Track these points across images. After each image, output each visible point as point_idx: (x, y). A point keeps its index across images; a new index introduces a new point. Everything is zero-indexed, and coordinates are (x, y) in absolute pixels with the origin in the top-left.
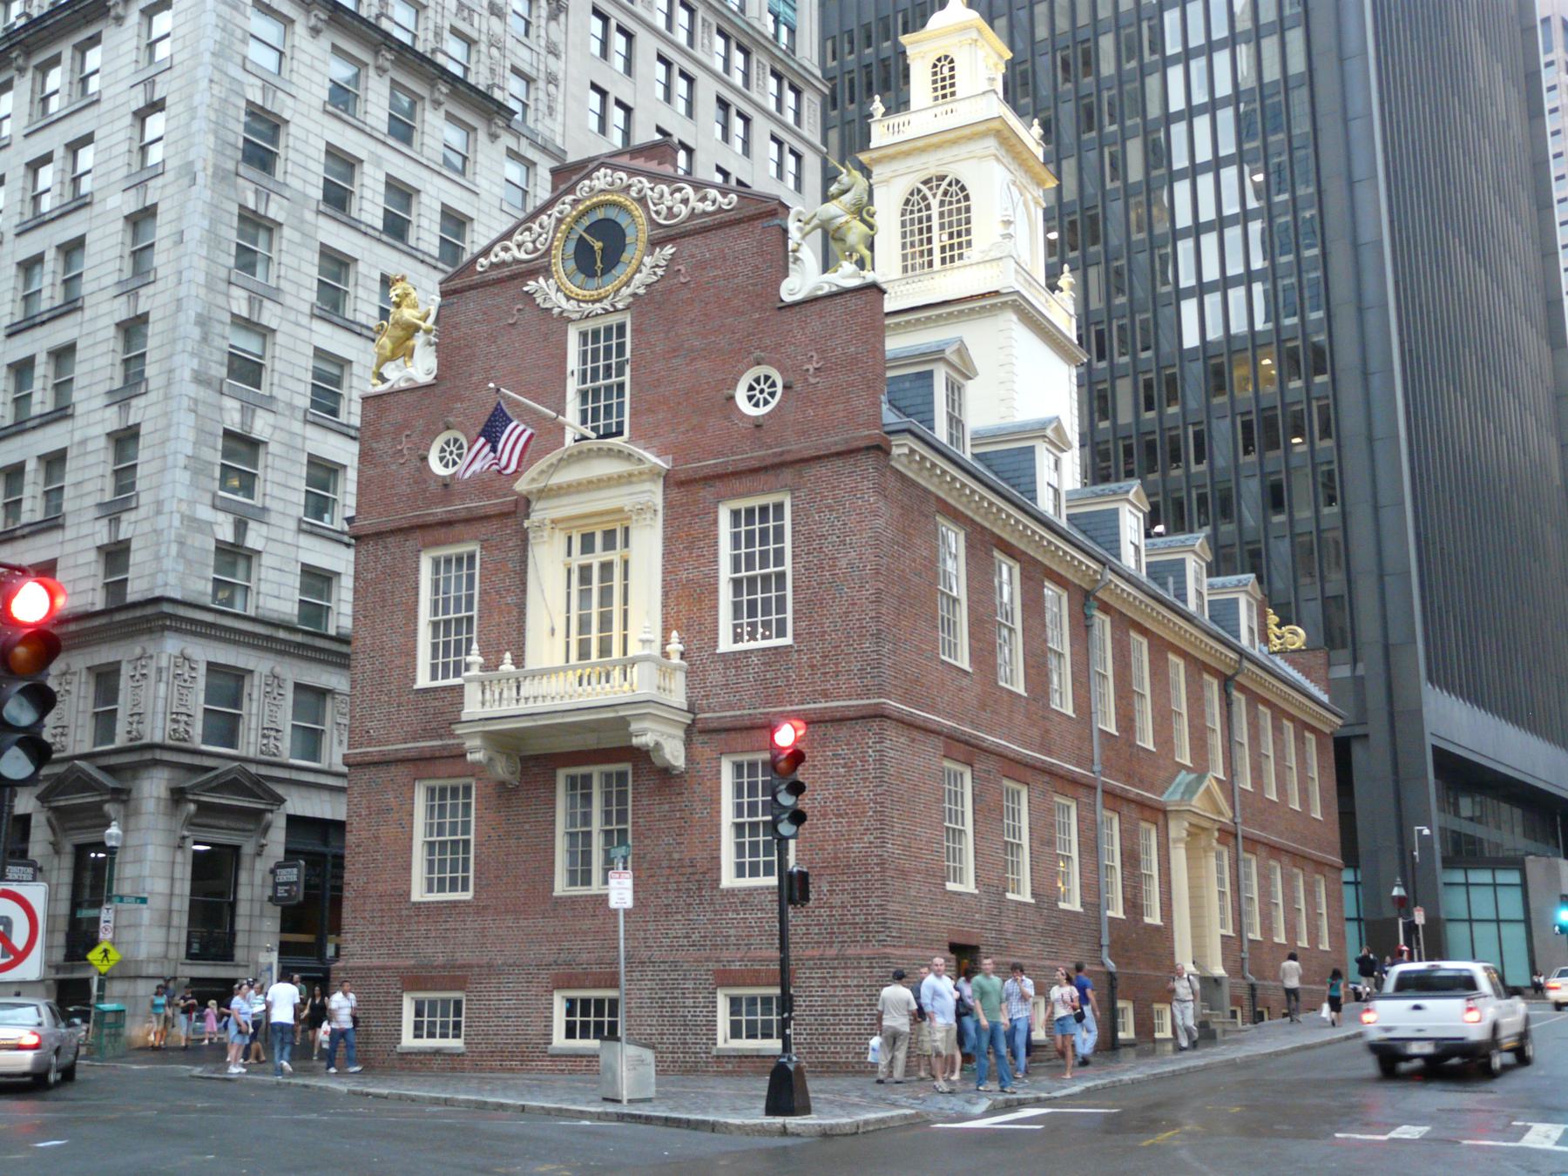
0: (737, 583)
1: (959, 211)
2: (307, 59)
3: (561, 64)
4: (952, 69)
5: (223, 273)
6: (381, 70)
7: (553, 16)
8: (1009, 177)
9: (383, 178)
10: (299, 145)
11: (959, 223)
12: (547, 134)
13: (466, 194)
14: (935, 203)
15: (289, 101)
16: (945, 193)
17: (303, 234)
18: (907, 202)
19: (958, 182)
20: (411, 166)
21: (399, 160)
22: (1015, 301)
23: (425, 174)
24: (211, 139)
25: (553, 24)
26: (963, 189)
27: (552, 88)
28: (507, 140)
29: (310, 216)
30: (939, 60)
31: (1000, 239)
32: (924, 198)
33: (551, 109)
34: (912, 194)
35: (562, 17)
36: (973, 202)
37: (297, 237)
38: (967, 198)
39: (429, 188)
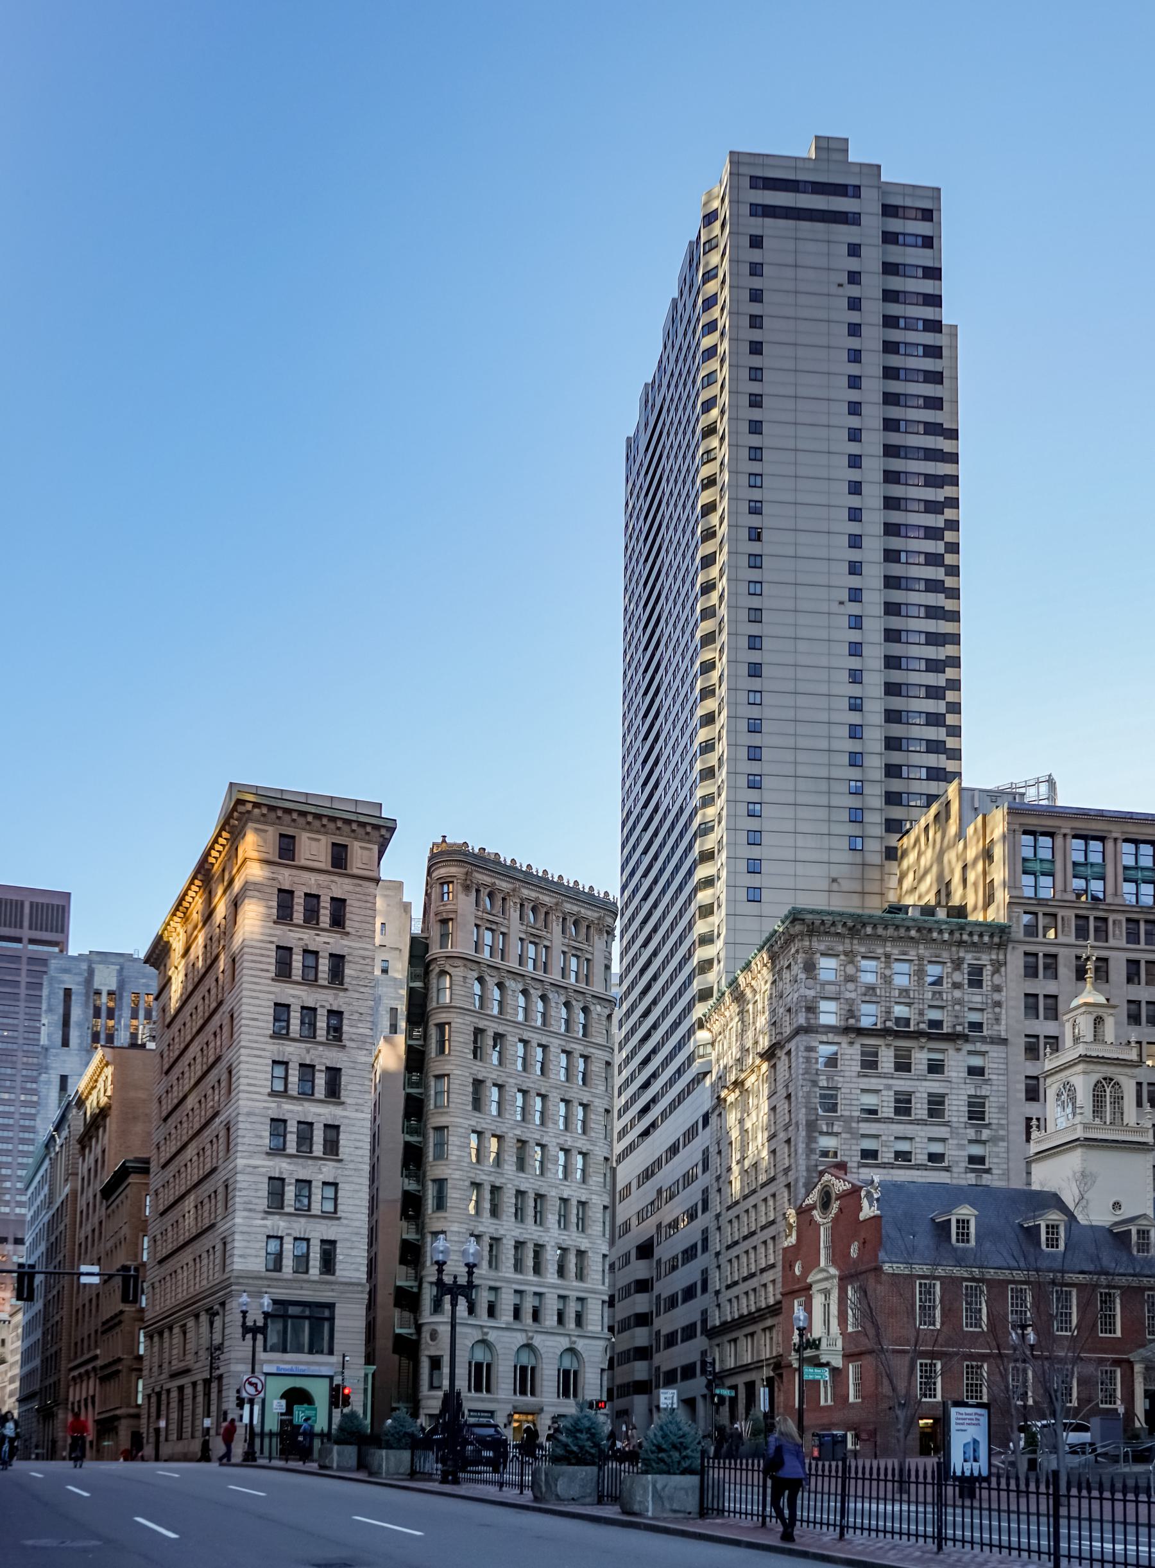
2: (848, 1057)
3: (1004, 994)
5: (813, 1163)
6: (888, 1046)
7: (996, 971)
9: (892, 1093)
10: (847, 1096)
12: (995, 1033)
13: (943, 1084)
15: (841, 1079)
17: (851, 1133)
20: (909, 1083)
21: (902, 1082)
23: (917, 1083)
24: (804, 1110)
25: (996, 976)
27: (997, 1010)
28: (969, 1047)
29: (854, 1125)
33: (997, 1019)
35: (1003, 969)
37: (848, 1136)
39: (920, 1089)
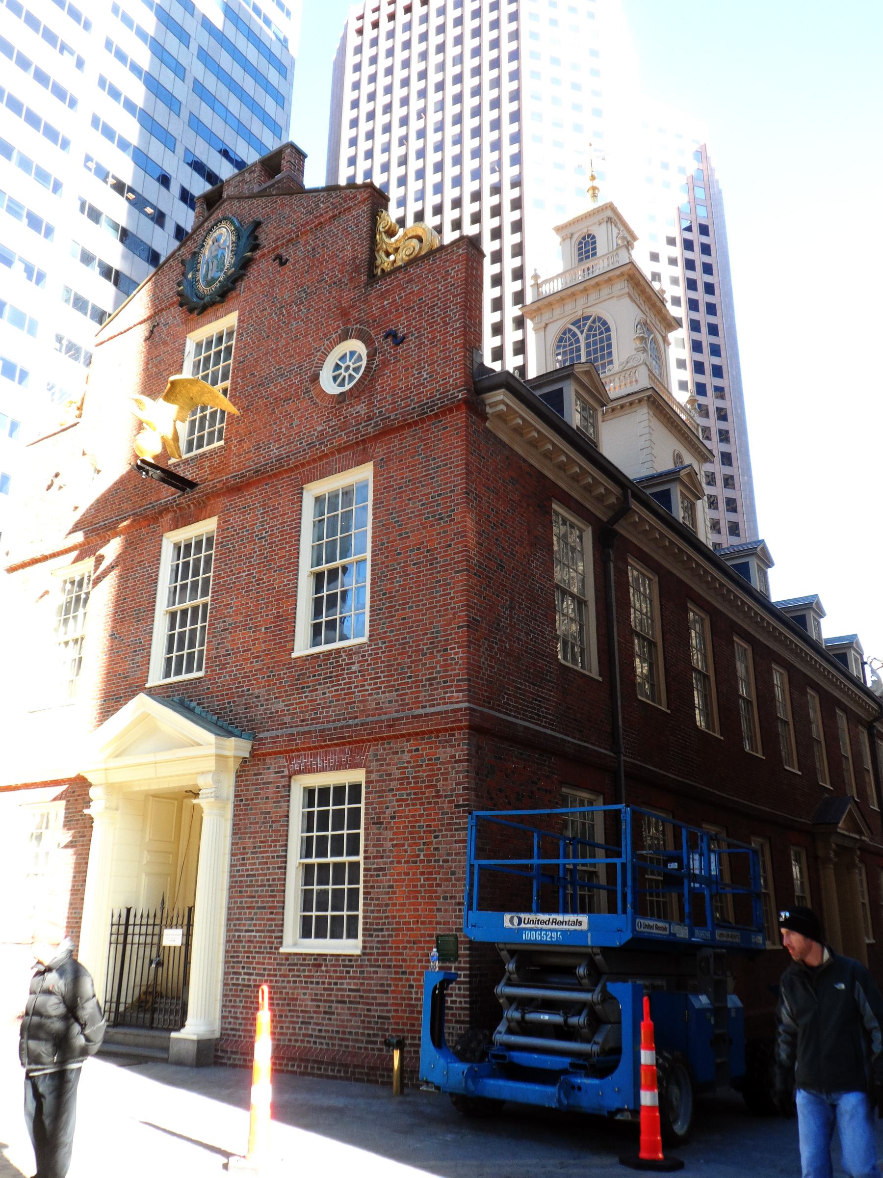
0: (319, 577)
1: (602, 341)
4: (595, 242)
8: (641, 315)
11: (602, 349)
14: (582, 338)
16: (590, 328)
18: (561, 340)
19: (600, 319)
22: (649, 397)
26: (605, 323)
30: (584, 238)
31: (635, 352)
32: (574, 335)
34: (565, 333)
36: (613, 333)
38: (608, 330)
